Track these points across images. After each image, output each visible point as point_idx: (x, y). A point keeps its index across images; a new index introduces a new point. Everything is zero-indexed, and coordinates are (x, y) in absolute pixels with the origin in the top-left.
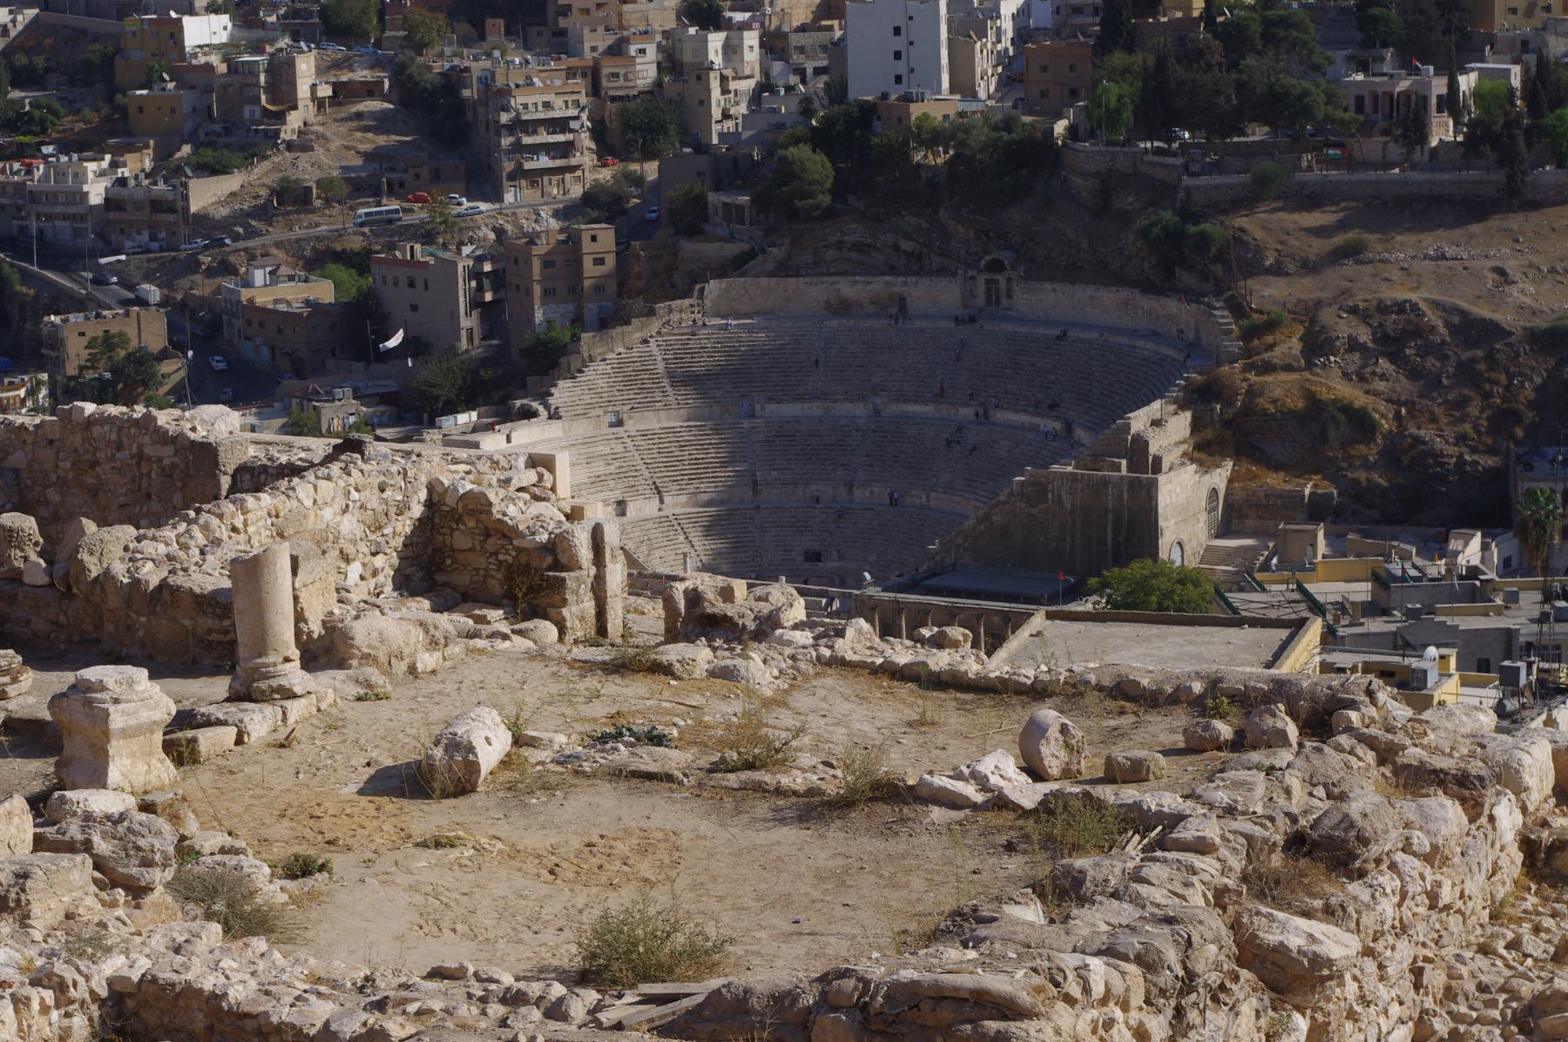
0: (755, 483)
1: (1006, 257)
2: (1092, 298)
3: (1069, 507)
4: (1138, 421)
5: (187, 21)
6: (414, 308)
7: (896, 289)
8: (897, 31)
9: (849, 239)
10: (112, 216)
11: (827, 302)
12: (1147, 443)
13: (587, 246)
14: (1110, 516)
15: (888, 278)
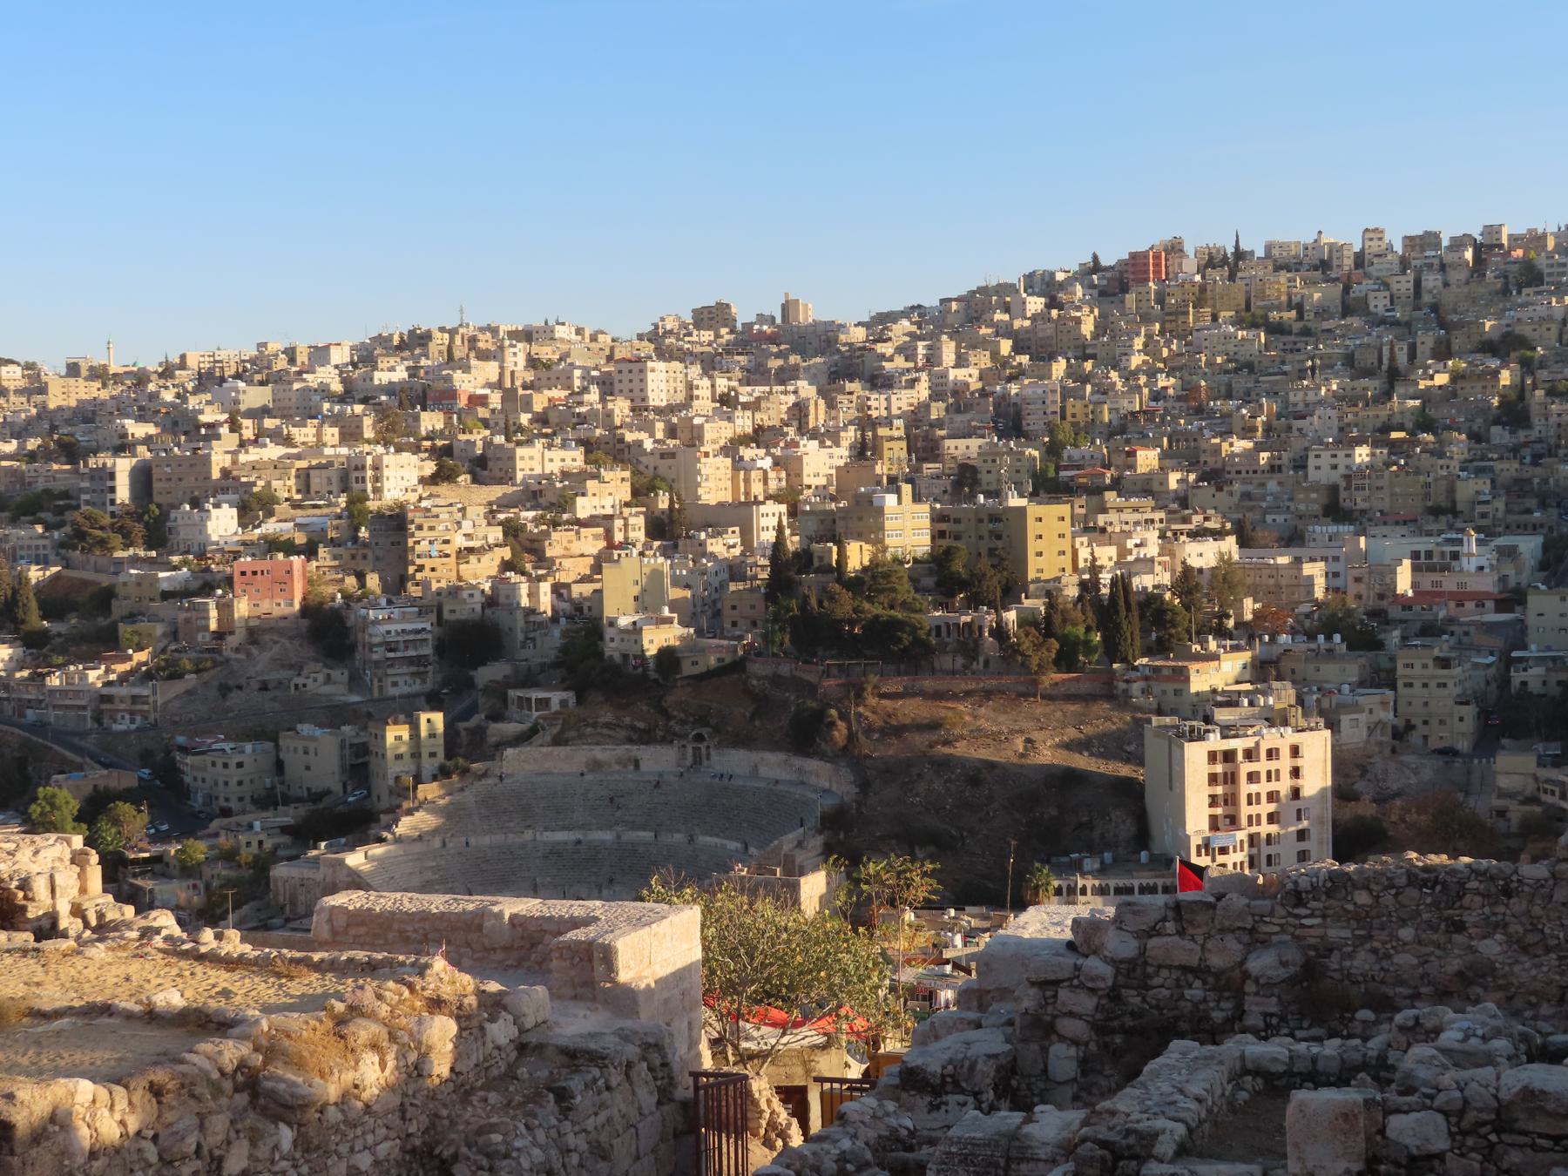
6: (308, 768)
9: (602, 720)
10: (104, 707)
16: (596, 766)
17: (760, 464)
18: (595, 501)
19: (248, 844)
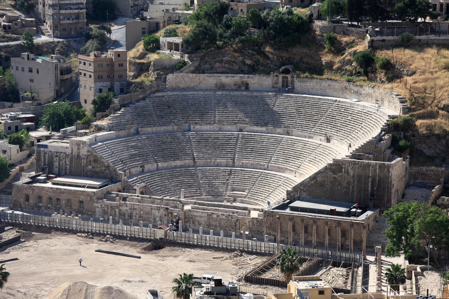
0: (194, 158)
1: (290, 67)
2: (329, 85)
3: (352, 175)
6: (32, 81)
7: (244, 80)
11: (216, 84)
14: (370, 179)
15: (241, 75)
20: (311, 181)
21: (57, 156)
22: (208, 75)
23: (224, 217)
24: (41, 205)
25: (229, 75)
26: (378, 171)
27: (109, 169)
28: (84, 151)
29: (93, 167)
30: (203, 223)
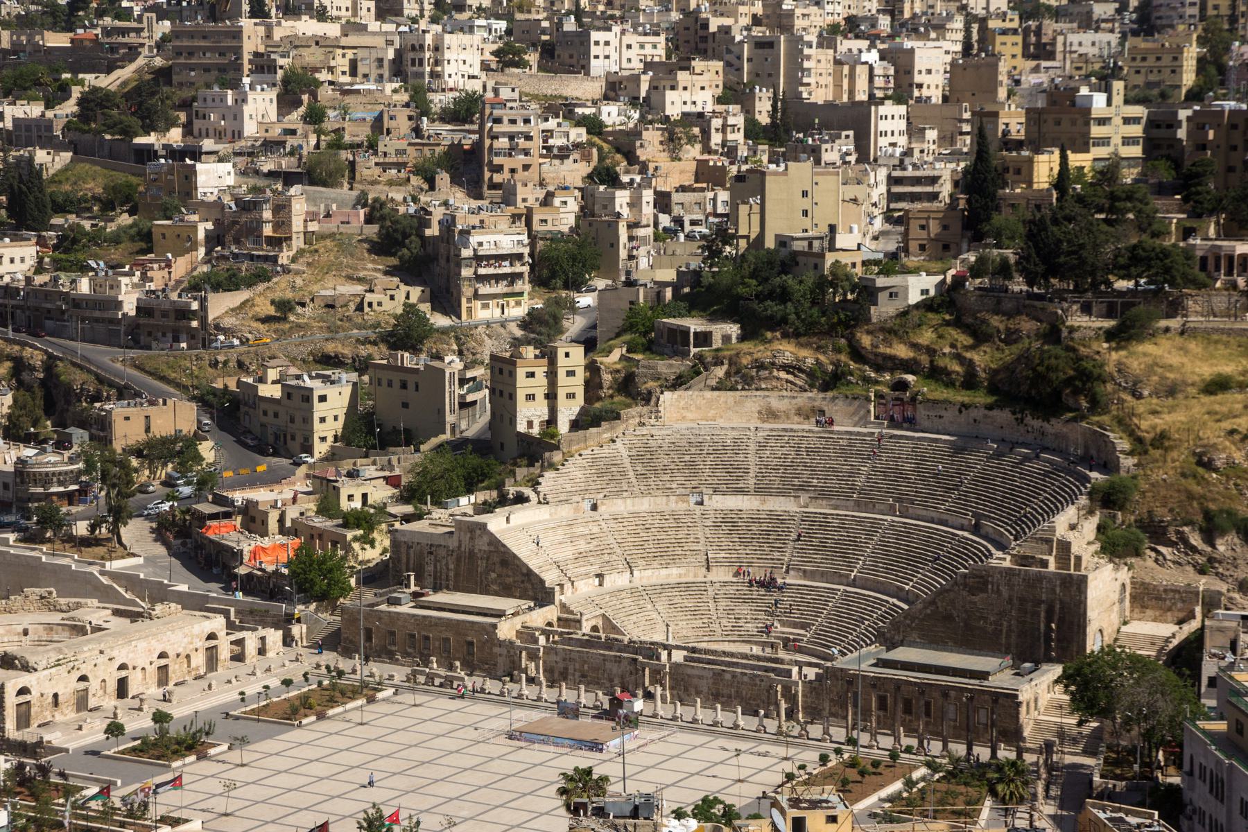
4: (1062, 522)
5: (199, 166)
6: (405, 405)
7: (816, 404)
8: (805, 194)
11: (760, 412)
12: (1069, 544)
13: (561, 360)
14: (1043, 607)
16: (770, 414)
17: (865, 57)
18: (686, 96)
19: (350, 497)
20: (925, 608)
21: (431, 553)
22: (743, 393)
23: (746, 679)
24: (394, 648)
25: (785, 393)
26: (1058, 590)
27: (529, 580)
28: (482, 544)
29: (499, 576)
30: (705, 689)
